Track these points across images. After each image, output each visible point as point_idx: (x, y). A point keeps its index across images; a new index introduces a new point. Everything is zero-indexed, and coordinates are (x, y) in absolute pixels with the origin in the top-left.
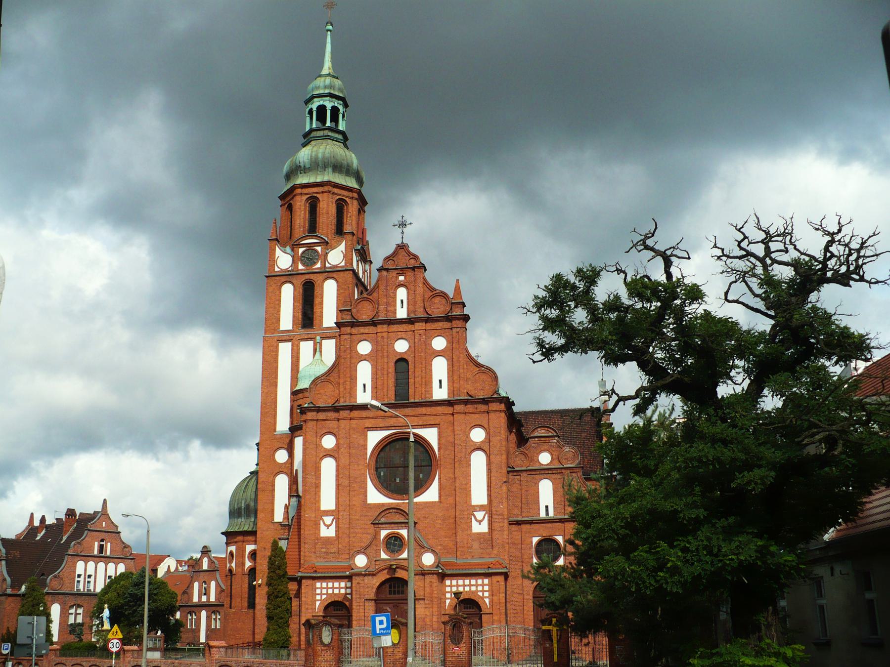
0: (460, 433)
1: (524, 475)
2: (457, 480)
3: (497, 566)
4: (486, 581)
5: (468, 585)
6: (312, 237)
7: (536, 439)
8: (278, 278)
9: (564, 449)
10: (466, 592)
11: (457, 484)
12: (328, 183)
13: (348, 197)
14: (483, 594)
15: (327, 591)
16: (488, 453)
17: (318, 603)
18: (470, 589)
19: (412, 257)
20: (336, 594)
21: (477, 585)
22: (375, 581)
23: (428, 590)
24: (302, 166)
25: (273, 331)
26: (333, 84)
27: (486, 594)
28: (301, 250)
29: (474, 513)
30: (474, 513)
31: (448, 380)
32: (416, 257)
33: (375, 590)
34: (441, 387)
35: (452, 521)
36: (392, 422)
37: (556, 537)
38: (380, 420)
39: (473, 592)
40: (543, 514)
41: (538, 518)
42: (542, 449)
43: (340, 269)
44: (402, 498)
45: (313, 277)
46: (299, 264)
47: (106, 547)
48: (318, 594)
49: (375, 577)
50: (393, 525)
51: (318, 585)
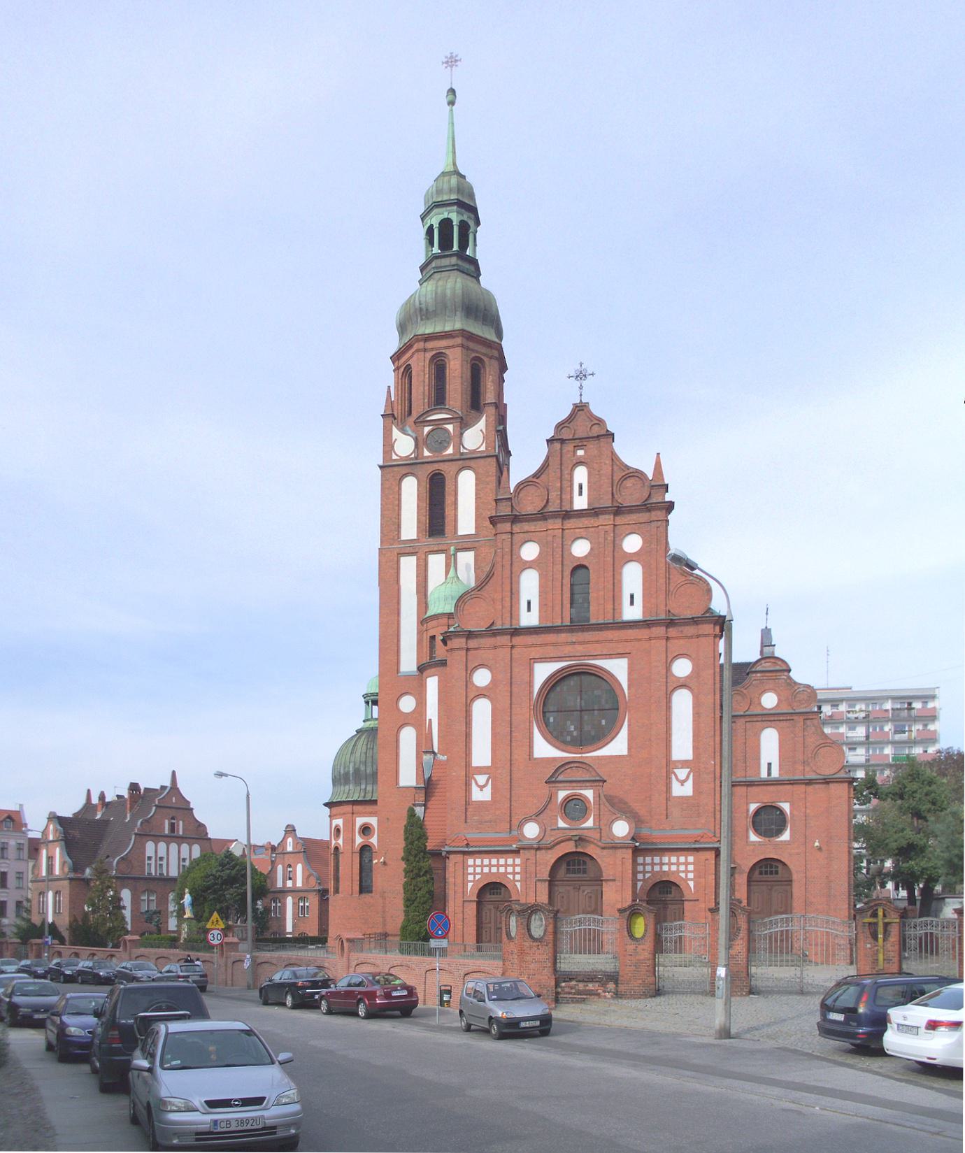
4: (691, 859)
6: (441, 411)
12: (464, 333)
13: (485, 355)
14: (686, 876)
15: (482, 870)
17: (470, 885)
18: (670, 869)
21: (678, 864)
22: (550, 856)
24: (425, 309)
27: (691, 876)
28: (427, 429)
29: (675, 770)
30: (675, 770)
33: (549, 868)
36: (568, 650)
38: (552, 648)
39: (673, 872)
42: (767, 687)
43: (479, 455)
44: (580, 751)
47: (178, 826)
48: (470, 874)
50: (574, 784)
51: (471, 862)
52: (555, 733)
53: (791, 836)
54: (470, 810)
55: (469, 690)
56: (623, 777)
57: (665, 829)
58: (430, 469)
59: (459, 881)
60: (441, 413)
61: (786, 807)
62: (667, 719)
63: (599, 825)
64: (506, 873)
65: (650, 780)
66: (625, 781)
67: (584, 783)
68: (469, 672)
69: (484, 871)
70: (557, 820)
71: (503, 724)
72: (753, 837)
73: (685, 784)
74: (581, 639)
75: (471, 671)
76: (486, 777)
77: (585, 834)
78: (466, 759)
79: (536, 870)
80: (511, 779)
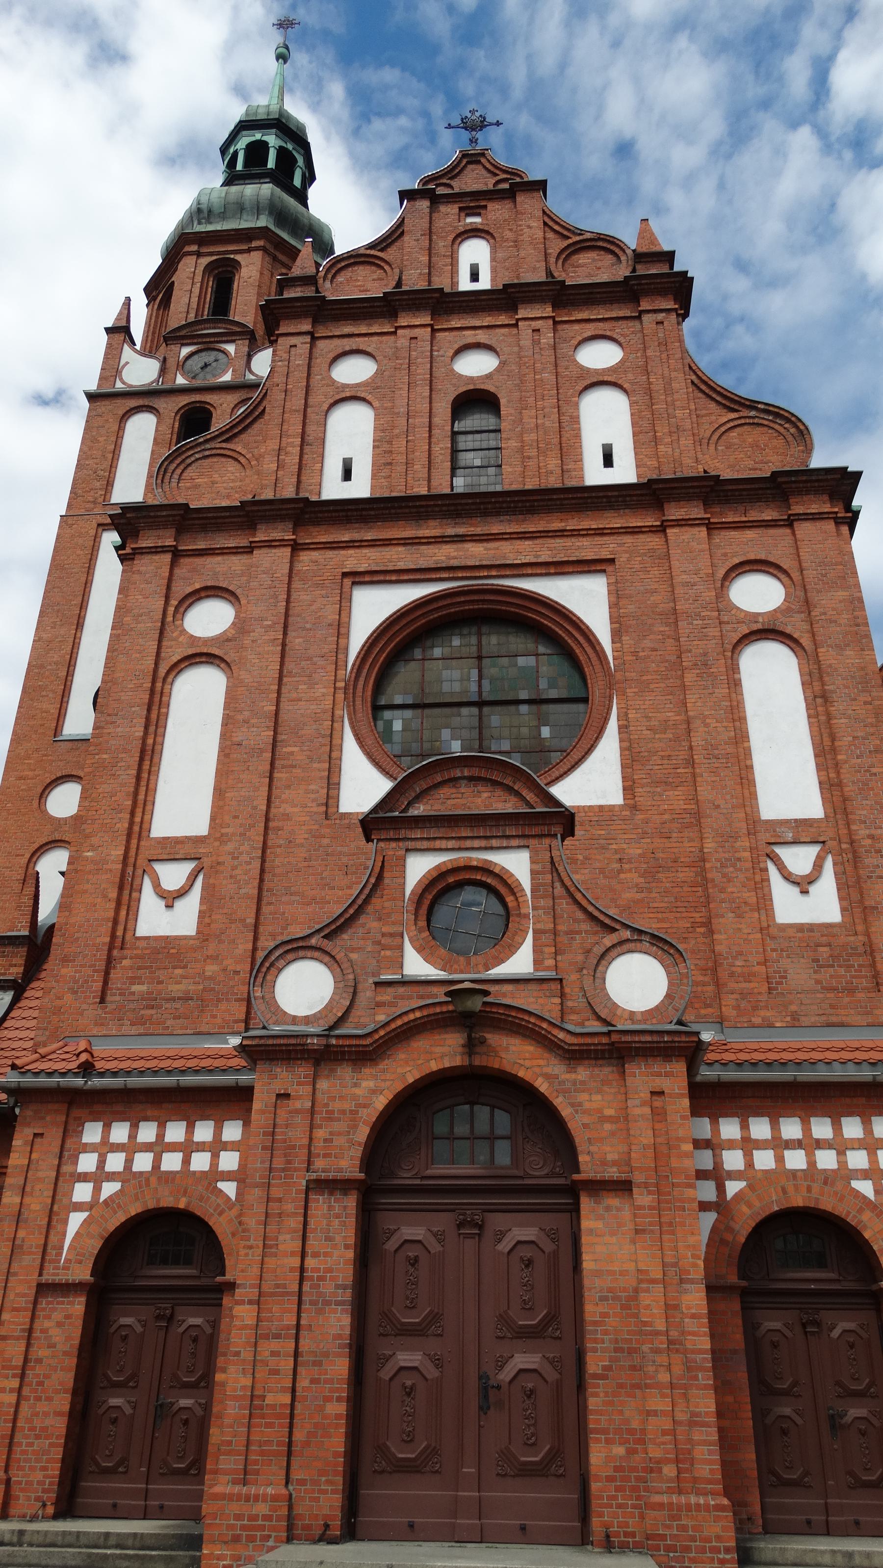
2: (697, 724)
8: (119, 401)
10: (794, 1173)
11: (697, 740)
15: (129, 1162)
16: (806, 641)
17: (76, 1220)
19: (505, 176)
20: (170, 1176)
21: (841, 1146)
22: (371, 1084)
23: (643, 1135)
28: (185, 351)
33: (363, 1133)
35: (686, 874)
38: (401, 549)
39: (828, 1177)
45: (208, 398)
48: (84, 1177)
49: (367, 1071)
55: (165, 643)
56: (616, 866)
57: (771, 1026)
58: (184, 400)
59: (37, 1204)
60: (215, 328)
64: (214, 1175)
66: (622, 876)
69: (136, 1168)
70: (401, 948)
73: (812, 889)
74: (478, 530)
75: (181, 602)
76: (187, 868)
78: (132, 814)
80: (262, 871)
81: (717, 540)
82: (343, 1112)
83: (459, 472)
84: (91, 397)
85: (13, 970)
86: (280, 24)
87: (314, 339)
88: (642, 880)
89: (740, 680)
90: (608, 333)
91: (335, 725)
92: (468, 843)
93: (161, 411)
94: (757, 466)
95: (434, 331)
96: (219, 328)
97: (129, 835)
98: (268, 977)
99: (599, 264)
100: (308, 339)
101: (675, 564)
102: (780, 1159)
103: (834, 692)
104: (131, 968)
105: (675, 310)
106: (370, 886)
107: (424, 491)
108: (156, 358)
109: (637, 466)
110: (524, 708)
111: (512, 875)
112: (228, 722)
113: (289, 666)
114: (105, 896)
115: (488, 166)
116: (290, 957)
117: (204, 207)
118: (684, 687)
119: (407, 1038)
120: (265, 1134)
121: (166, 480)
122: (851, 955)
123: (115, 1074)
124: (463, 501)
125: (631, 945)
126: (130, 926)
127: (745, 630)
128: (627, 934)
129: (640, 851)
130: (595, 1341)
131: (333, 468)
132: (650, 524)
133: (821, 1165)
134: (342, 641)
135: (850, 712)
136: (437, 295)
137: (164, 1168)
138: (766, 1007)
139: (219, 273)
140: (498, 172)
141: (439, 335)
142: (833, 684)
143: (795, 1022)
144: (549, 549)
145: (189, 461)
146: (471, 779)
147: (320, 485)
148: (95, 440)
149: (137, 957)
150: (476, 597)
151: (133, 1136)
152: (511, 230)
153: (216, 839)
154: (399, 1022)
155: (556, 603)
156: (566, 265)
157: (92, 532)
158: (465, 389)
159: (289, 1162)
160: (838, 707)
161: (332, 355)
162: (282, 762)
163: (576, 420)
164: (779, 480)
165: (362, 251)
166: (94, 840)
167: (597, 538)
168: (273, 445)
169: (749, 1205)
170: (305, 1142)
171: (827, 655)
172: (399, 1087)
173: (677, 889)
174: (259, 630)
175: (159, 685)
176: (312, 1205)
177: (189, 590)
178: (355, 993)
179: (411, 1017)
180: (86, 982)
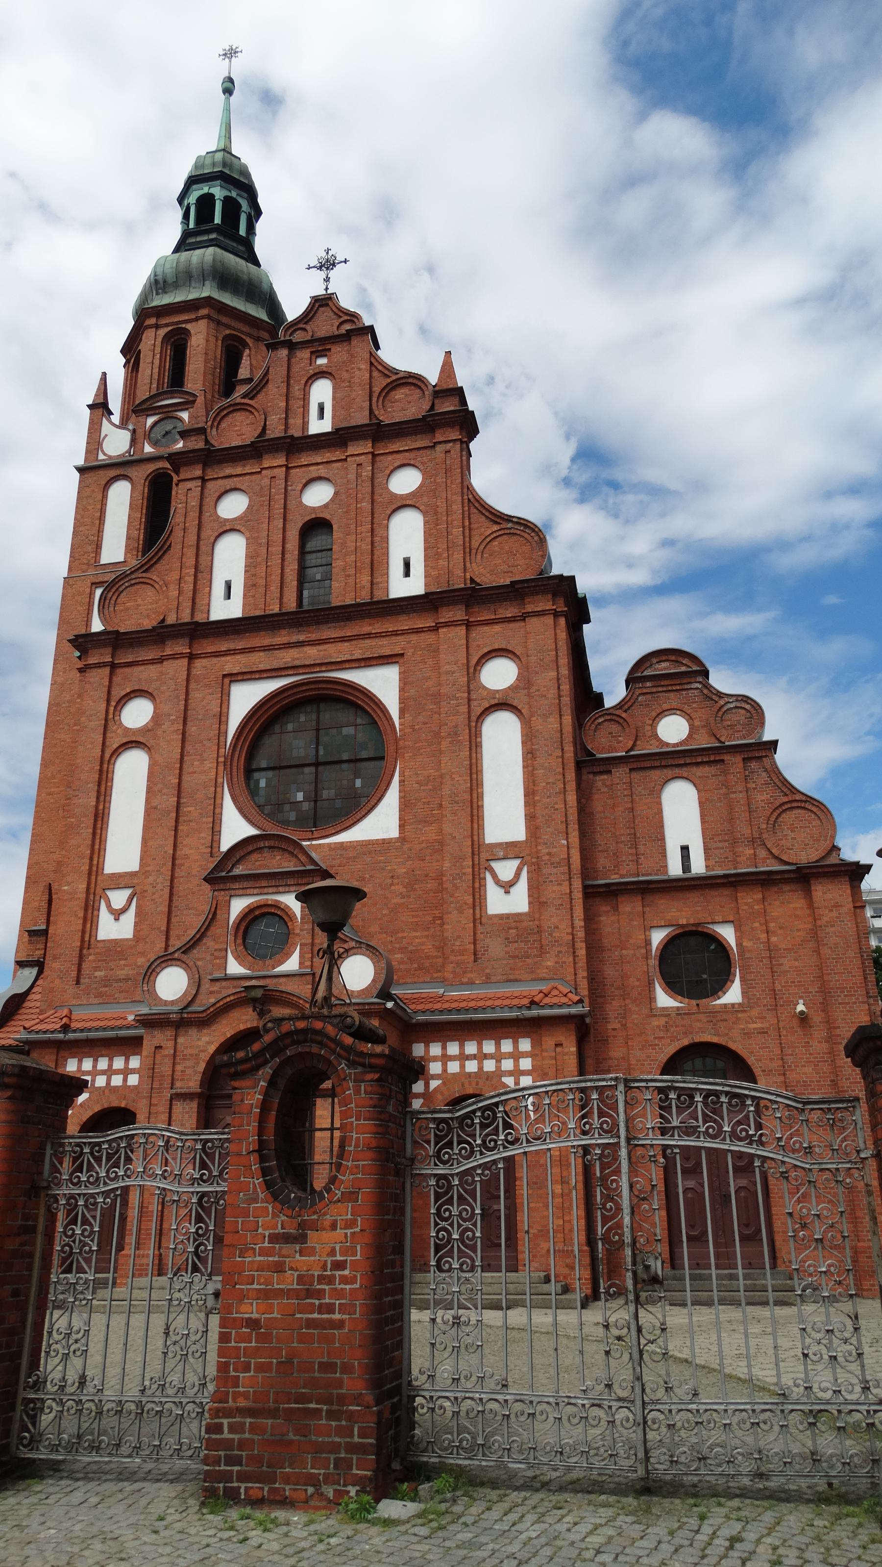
0: (455, 668)
1: (620, 773)
3: (555, 1000)
4: (525, 1045)
5: (473, 1057)
7: (648, 684)
8: (101, 472)
9: (722, 702)
10: (470, 1074)
11: (446, 791)
19: (346, 318)
21: (498, 1057)
22: (207, 1039)
24: (161, 282)
25: (85, 567)
26: (229, 161)
28: (150, 421)
29: (494, 864)
30: (494, 864)
31: (426, 556)
32: (353, 317)
33: (202, 1066)
34: (407, 574)
35: (432, 885)
36: (289, 657)
37: (710, 926)
38: (262, 654)
39: (489, 1076)
40: (675, 869)
41: (666, 877)
44: (309, 835)
46: (146, 445)
49: (205, 1031)
50: (264, 883)
52: (268, 809)
53: (744, 993)
54: (90, 959)
55: (109, 735)
56: (389, 881)
61: (728, 933)
62: (471, 765)
63: (312, 966)
65: (441, 884)
66: (393, 887)
67: (279, 880)
68: (113, 704)
70: (226, 957)
71: (165, 791)
72: (664, 1000)
73: (512, 890)
74: (314, 636)
76: (126, 893)
77: (281, 988)
78: (91, 859)
79: (173, 1071)
81: (473, 634)
82: (191, 1055)
83: (306, 585)
84: (81, 470)
85: (38, 952)
86: (225, 55)
87: (204, 480)
88: (405, 890)
89: (481, 742)
90: (412, 462)
91: (218, 789)
92: (266, 890)
93: (134, 478)
94: (511, 569)
95: (288, 468)
96: (175, 398)
97: (90, 874)
98: (152, 978)
99: (410, 399)
100: (199, 483)
101: (442, 656)
102: (462, 1066)
103: (538, 750)
104: (95, 961)
105: (460, 440)
106: (208, 920)
107: (276, 610)
108: (128, 430)
109: (426, 577)
110: (345, 766)
111: (291, 909)
112: (149, 791)
113: (188, 747)
114: (76, 916)
115: (334, 308)
116: (163, 965)
117: (160, 278)
118: (441, 751)
119: (227, 1012)
120: (149, 1069)
121: (106, 606)
122: (529, 934)
123: (82, 1031)
124: (302, 616)
125: (355, 950)
126: (93, 933)
127: (486, 704)
128: (353, 944)
129: (405, 870)
130: (319, 1174)
131: (218, 589)
132: (428, 625)
133: (485, 1069)
134: (223, 727)
135: (547, 764)
136: (289, 440)
137: (112, 1084)
138: (471, 972)
139: (175, 340)
140: (341, 314)
141: (293, 471)
142: (538, 744)
143: (488, 980)
144: (361, 648)
145: (121, 589)
146: (270, 847)
147: (209, 605)
148: (85, 509)
149: (98, 953)
150: (313, 686)
151: (95, 1066)
152: (347, 371)
153: (143, 874)
154: (221, 1003)
155: (365, 688)
156: (386, 402)
157: (88, 590)
158: (308, 518)
159: (161, 1084)
160: (540, 761)
161: (217, 494)
162: (185, 818)
163: (386, 539)
164: (517, 586)
165: (239, 400)
166: (69, 879)
167: (394, 638)
168: (175, 576)
169: (442, 1094)
170: (170, 1073)
171: (537, 723)
172: (222, 1039)
173: (424, 896)
174: (168, 723)
175: (105, 766)
176: (174, 1107)
177: (123, 693)
178: (199, 986)
179: (228, 999)
180: (67, 971)
